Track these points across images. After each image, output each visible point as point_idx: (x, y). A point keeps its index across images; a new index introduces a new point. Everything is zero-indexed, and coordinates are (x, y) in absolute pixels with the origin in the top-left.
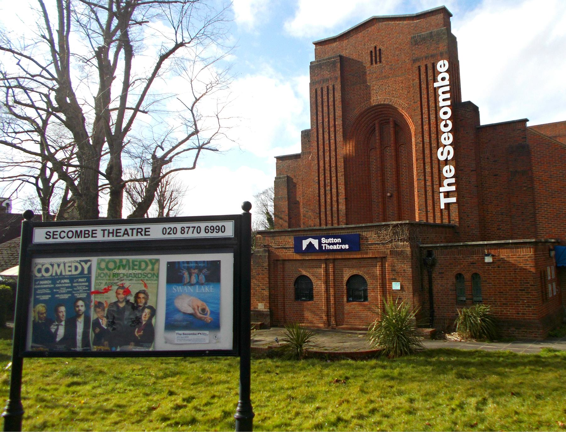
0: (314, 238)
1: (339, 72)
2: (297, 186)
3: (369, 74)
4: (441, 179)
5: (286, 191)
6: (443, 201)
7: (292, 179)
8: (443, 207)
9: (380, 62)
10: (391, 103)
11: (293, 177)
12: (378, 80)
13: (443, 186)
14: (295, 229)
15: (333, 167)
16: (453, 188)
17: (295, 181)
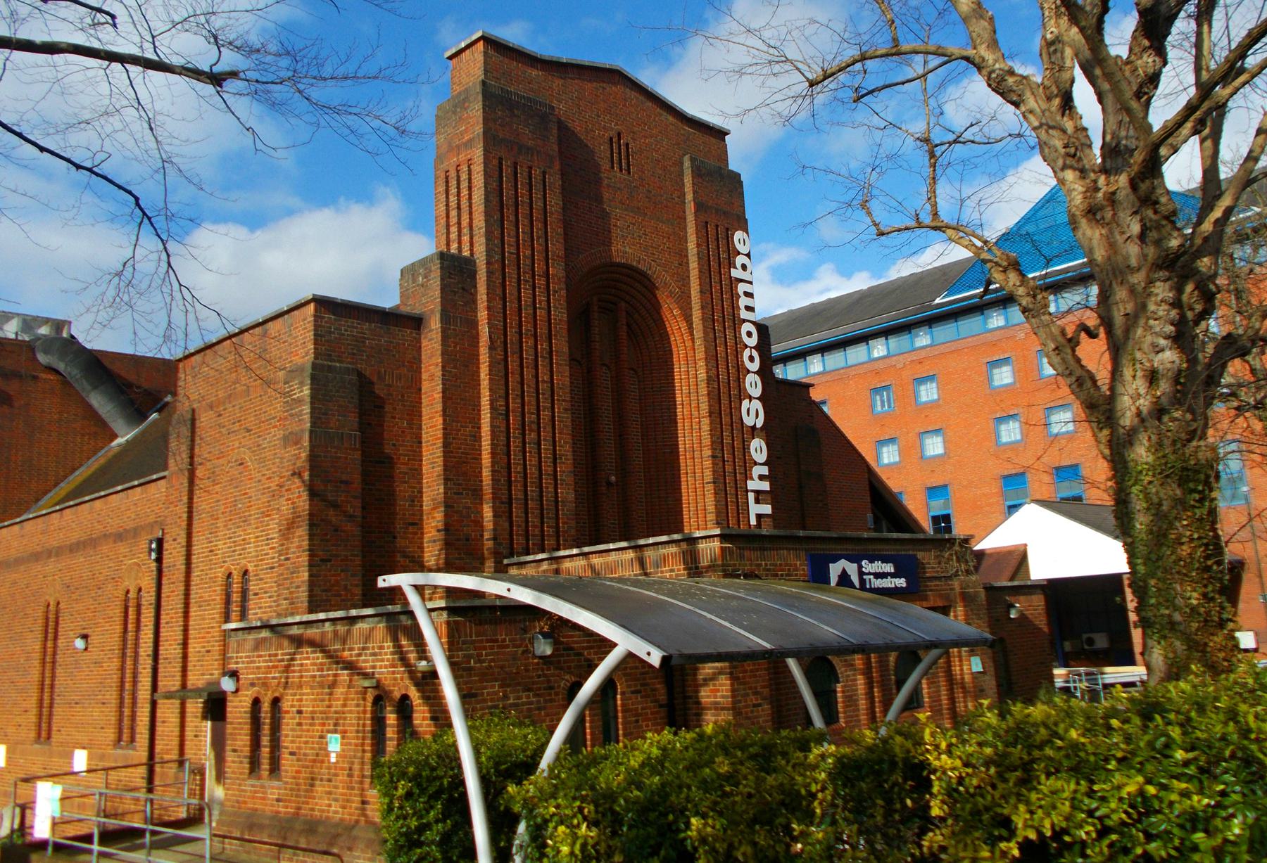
0: (851, 559)
1: (556, 148)
2: (388, 408)
3: (609, 186)
4: (749, 463)
5: (353, 418)
6: (755, 509)
7: (373, 383)
8: (753, 521)
9: (629, 173)
10: (649, 272)
11: (375, 379)
12: (626, 210)
13: (752, 479)
14: (818, 533)
15: (543, 381)
16: (766, 486)
17: (379, 390)
